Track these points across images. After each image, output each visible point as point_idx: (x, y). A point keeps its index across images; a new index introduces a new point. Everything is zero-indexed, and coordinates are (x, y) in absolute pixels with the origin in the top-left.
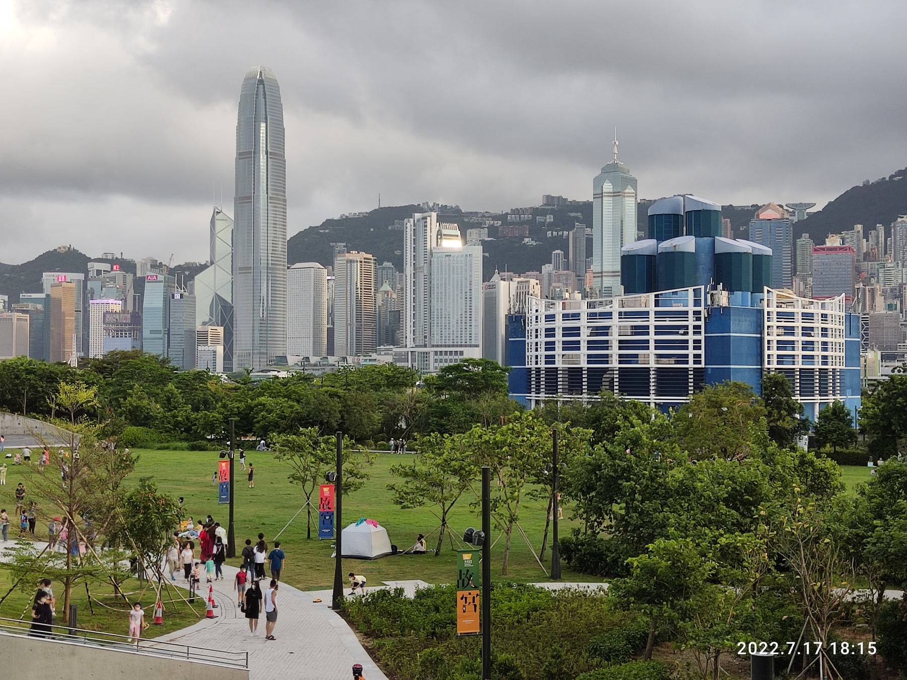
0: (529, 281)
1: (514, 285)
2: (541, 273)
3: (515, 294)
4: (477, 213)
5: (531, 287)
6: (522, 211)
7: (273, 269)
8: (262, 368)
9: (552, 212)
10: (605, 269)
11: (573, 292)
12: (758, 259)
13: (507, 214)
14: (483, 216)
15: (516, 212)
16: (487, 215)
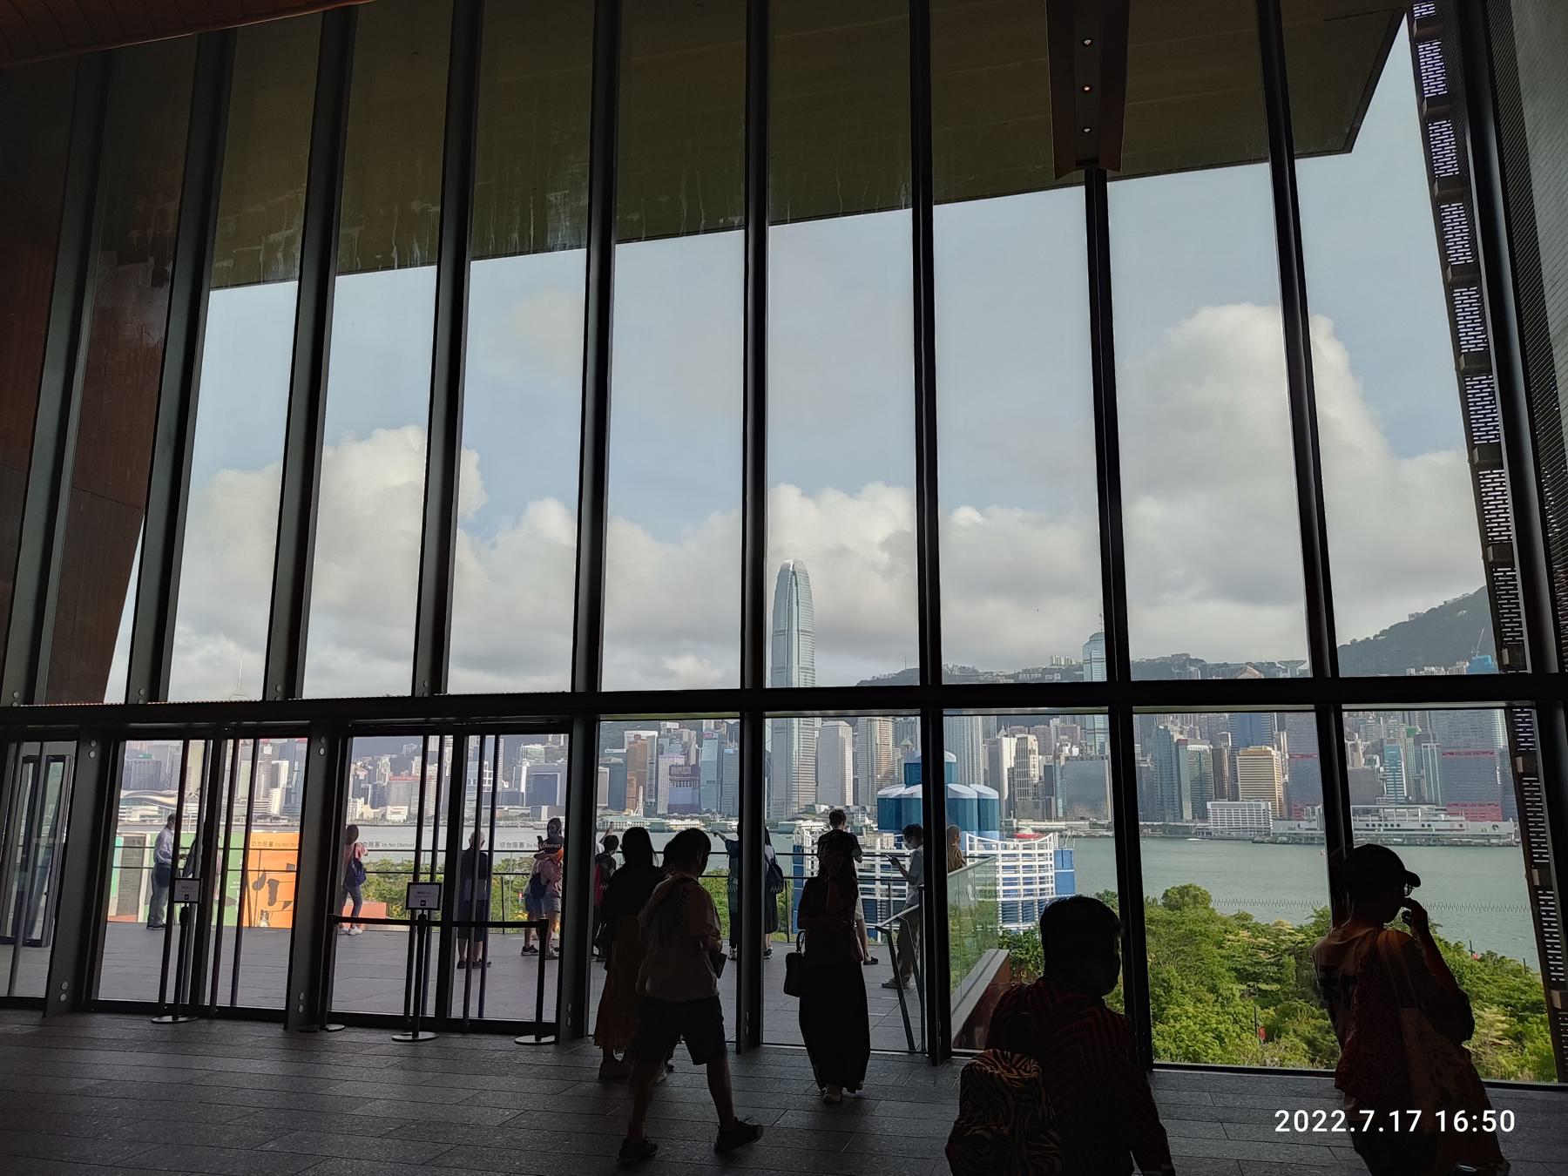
0: (1027, 738)
1: (1014, 741)
2: (1049, 726)
3: (1015, 750)
4: (992, 673)
5: (1029, 743)
6: (1034, 671)
7: (803, 728)
8: (790, 816)
9: (1059, 671)
10: (1096, 727)
11: (1072, 746)
12: (982, 802)
13: (1019, 673)
14: (998, 675)
15: (1025, 671)
16: (1001, 674)
